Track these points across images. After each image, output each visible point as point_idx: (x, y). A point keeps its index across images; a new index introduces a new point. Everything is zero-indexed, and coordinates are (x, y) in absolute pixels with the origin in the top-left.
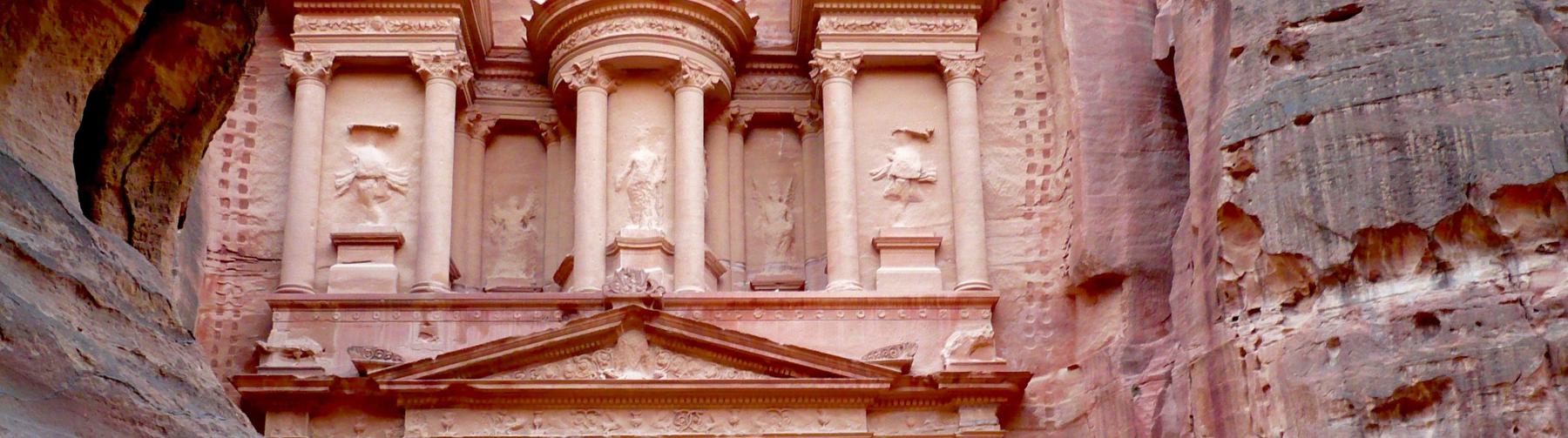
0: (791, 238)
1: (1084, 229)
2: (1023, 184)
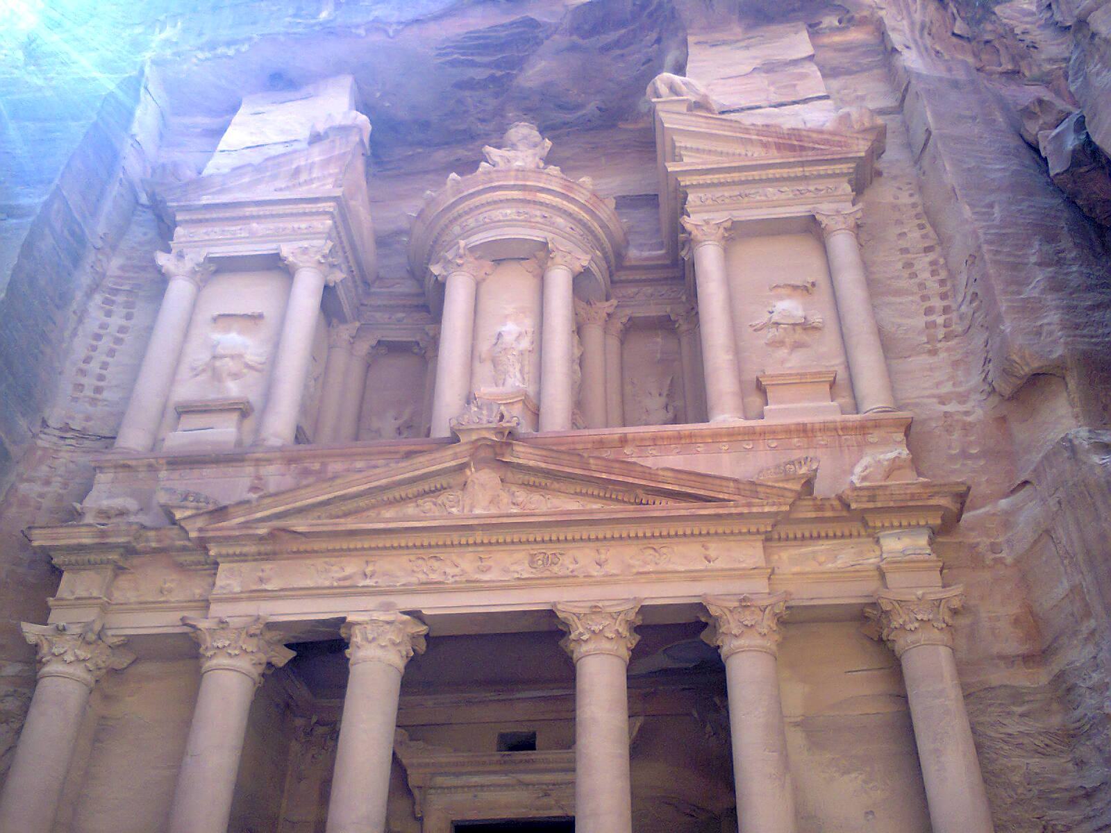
1: (1007, 327)
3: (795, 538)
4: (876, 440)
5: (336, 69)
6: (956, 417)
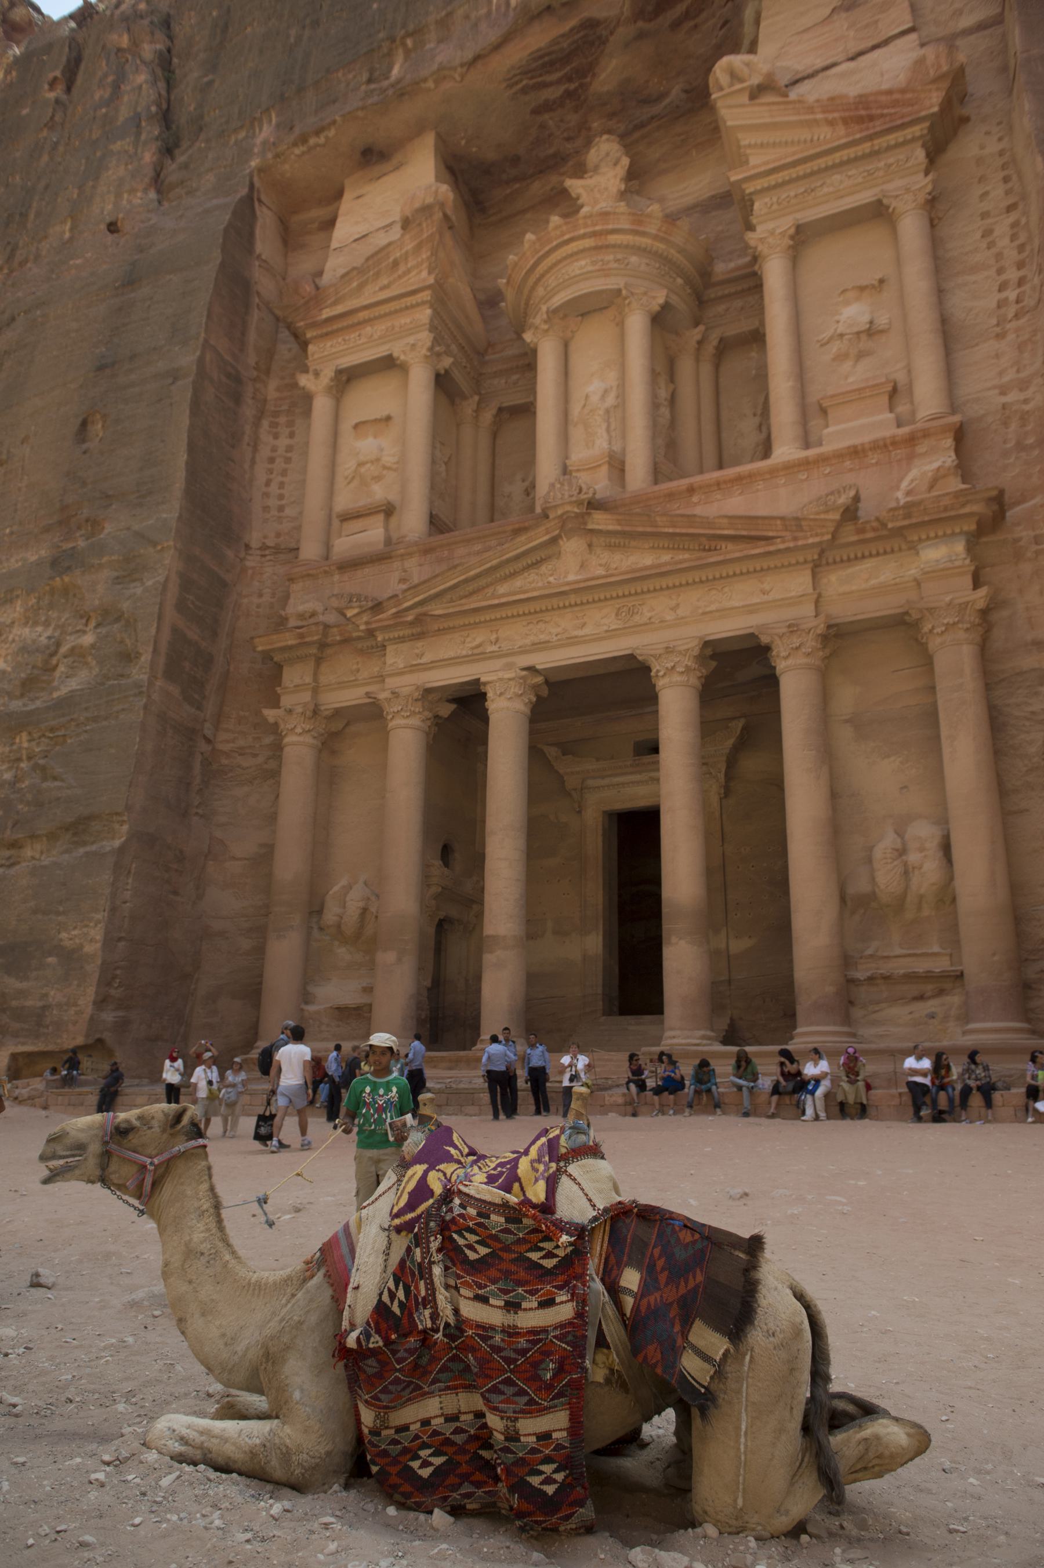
2: (994, 305)
3: (842, 561)
4: (925, 450)
5: (418, 130)
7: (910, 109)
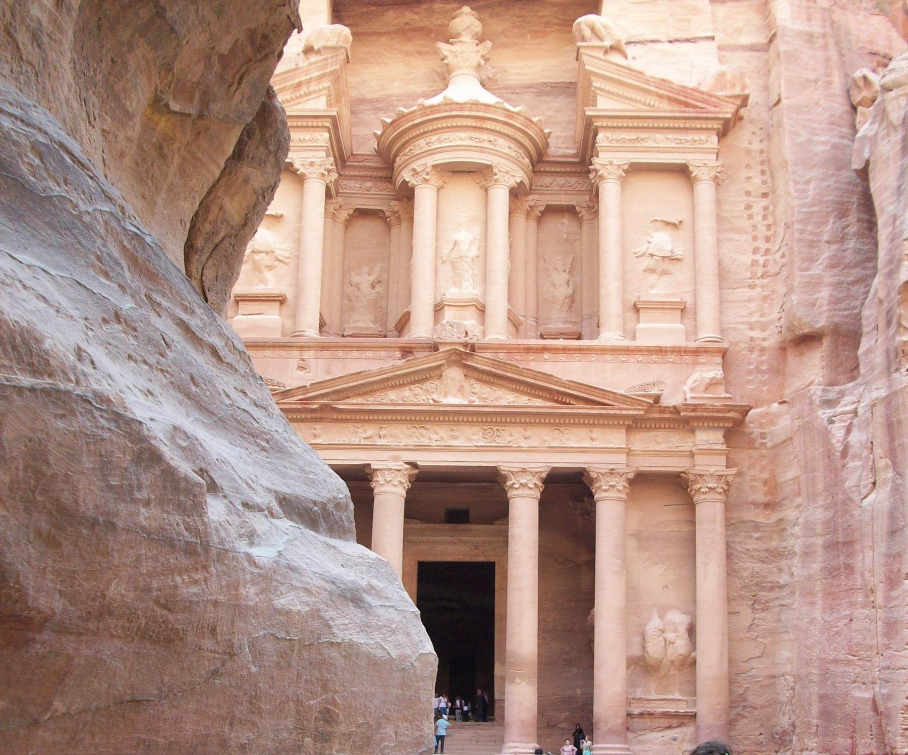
0: (572, 299)
1: (795, 298)
2: (749, 263)
4: (703, 361)
6: (757, 342)
7: (712, 109)
